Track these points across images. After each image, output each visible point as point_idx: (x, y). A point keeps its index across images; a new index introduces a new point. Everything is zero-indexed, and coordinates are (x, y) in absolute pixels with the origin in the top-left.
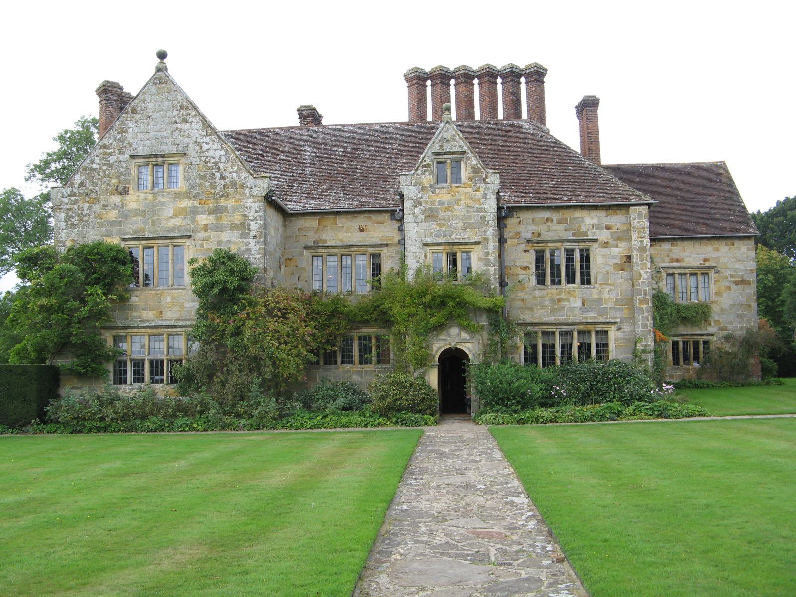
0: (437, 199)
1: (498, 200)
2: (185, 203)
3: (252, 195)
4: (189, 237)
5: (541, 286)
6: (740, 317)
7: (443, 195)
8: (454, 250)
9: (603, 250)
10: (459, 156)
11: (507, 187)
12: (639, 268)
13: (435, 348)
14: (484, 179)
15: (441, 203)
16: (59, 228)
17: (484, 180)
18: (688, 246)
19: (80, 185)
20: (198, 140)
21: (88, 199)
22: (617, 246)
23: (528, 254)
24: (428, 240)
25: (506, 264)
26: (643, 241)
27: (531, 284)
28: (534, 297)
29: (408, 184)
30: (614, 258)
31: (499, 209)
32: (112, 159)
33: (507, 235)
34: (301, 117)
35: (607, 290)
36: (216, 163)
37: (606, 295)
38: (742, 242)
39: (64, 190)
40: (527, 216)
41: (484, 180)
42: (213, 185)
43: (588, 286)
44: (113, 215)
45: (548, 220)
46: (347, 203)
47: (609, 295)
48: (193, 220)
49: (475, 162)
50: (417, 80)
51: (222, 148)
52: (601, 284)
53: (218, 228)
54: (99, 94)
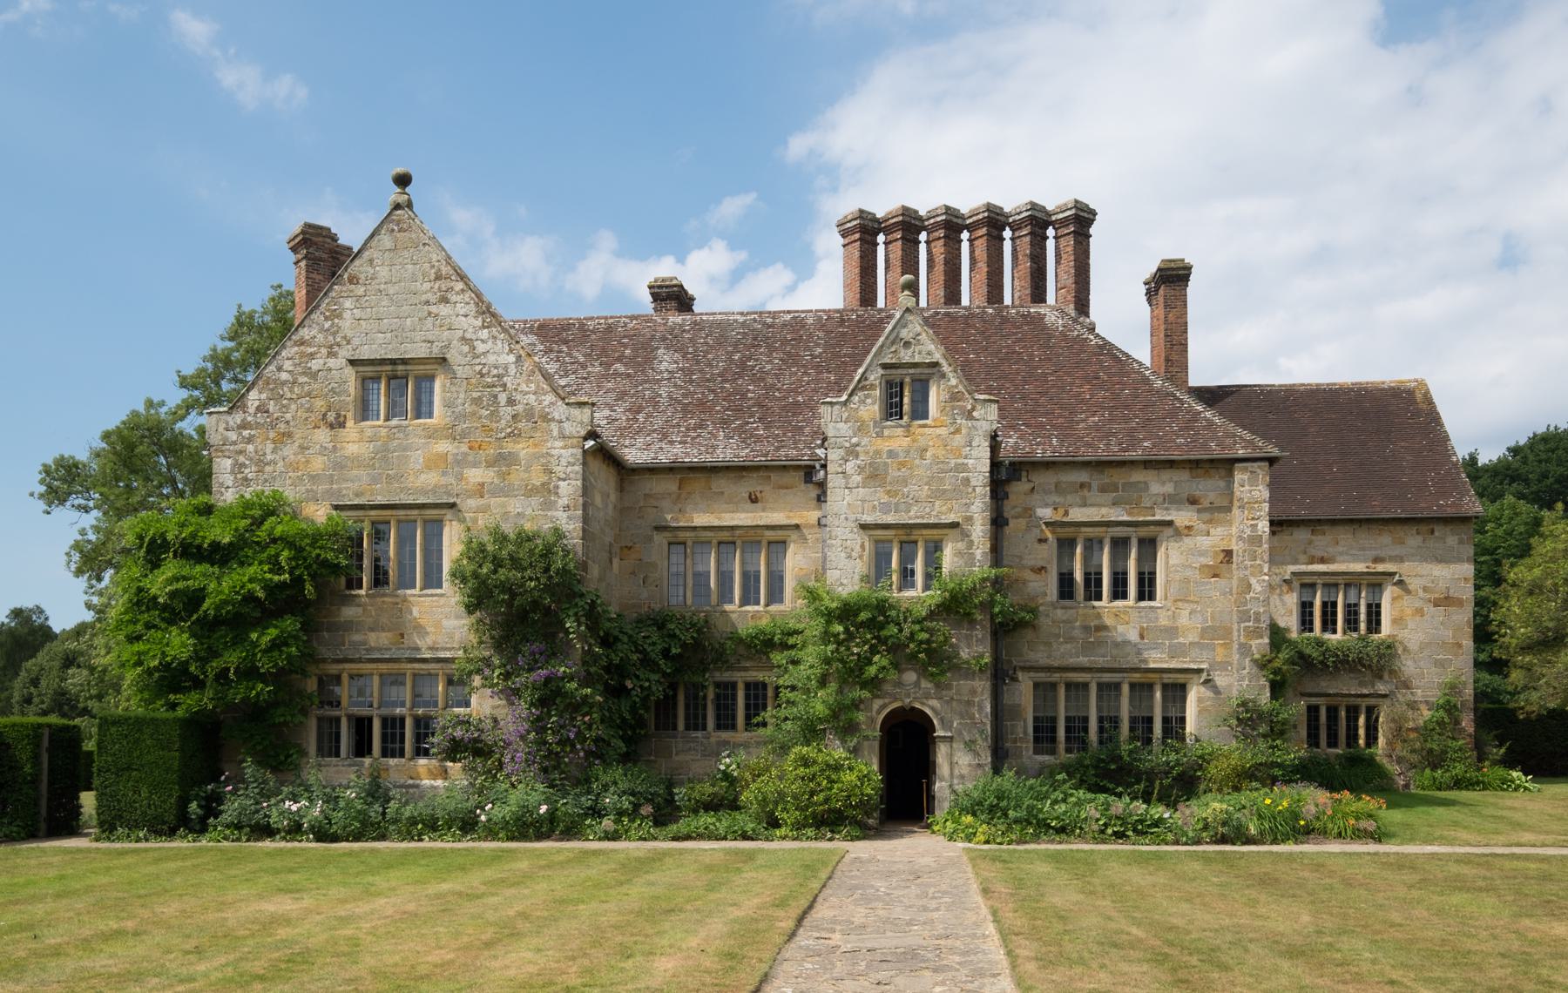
0: (885, 446)
1: (995, 446)
2: (443, 446)
3: (563, 437)
4: (453, 506)
5: (1067, 603)
6: (1440, 664)
7: (896, 438)
10: (927, 371)
11: (1012, 427)
14: (970, 412)
15: (891, 454)
16: (222, 485)
17: (969, 415)
19: (258, 409)
20: (468, 336)
21: (272, 434)
22: (1208, 534)
23: (1045, 546)
24: (868, 519)
27: (1049, 599)
29: (834, 421)
31: (995, 465)
32: (315, 365)
34: (656, 297)
35: (1186, 613)
36: (499, 376)
37: (1184, 620)
38: (1448, 529)
39: (229, 418)
41: (969, 415)
42: (494, 415)
43: (1152, 604)
44: (318, 464)
45: (1082, 485)
46: (727, 450)
47: (1189, 623)
48: (460, 477)
49: (954, 382)
51: (511, 351)
53: (504, 491)
54: (294, 249)
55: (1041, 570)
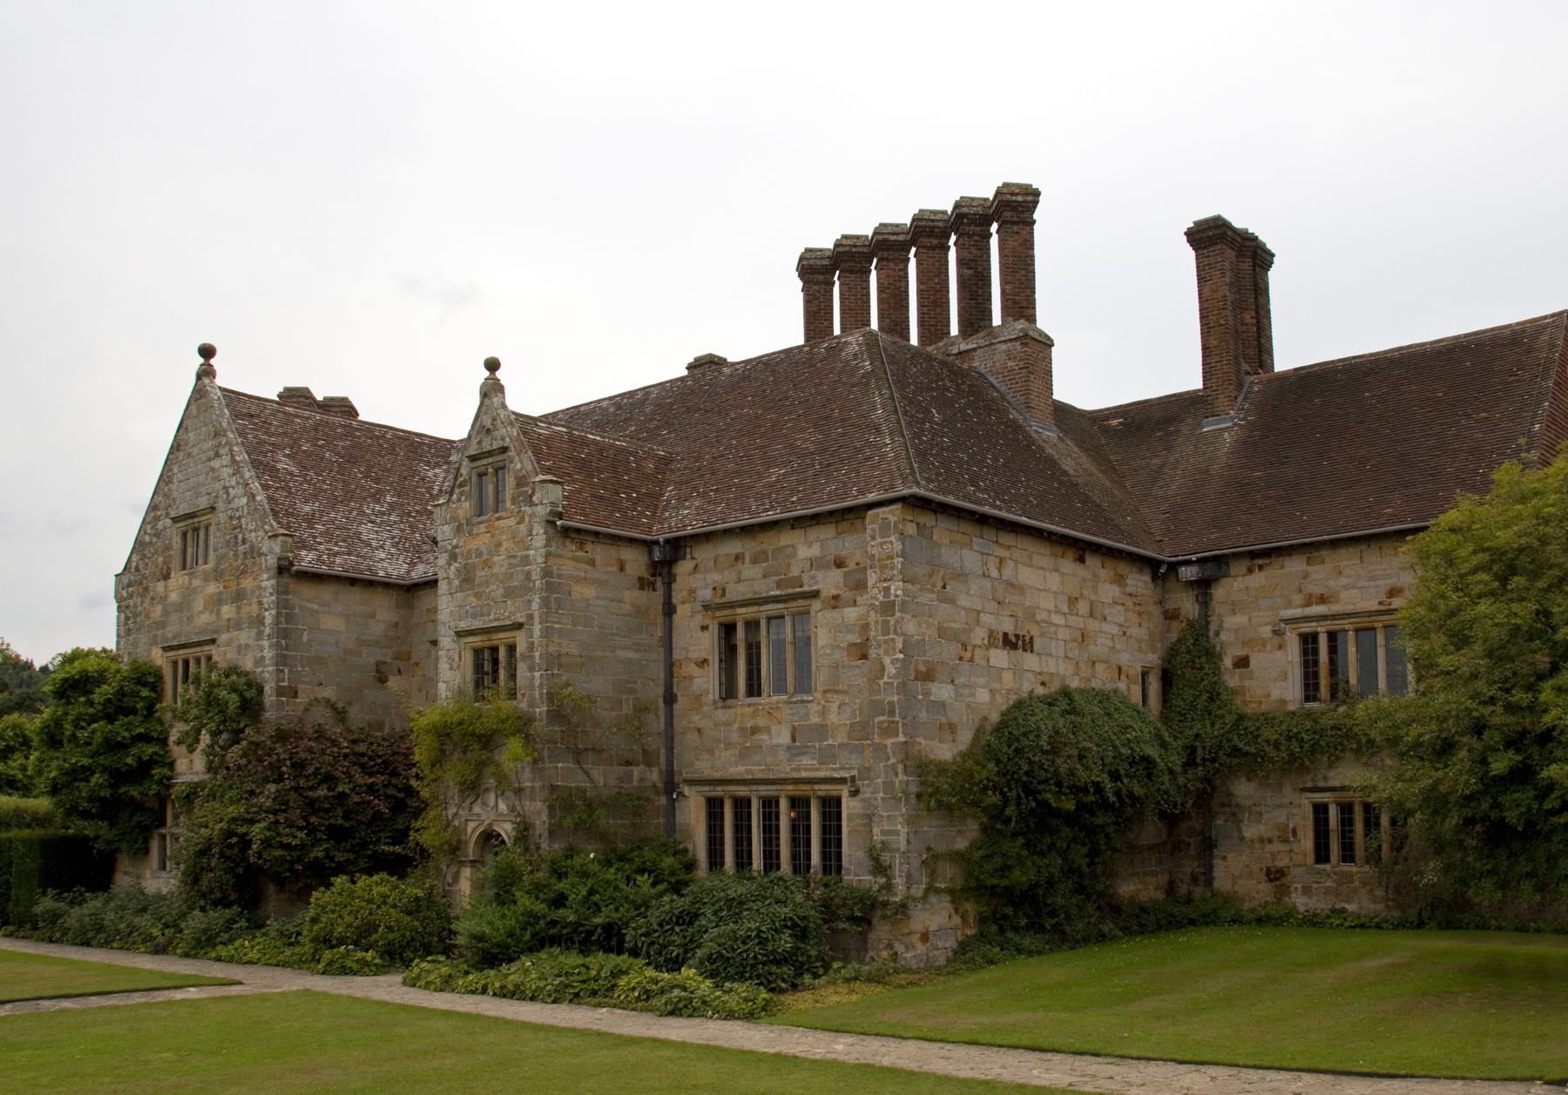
0: (474, 544)
4: (213, 641)
12: (881, 652)
13: (469, 830)
14: (531, 497)
18: (1347, 559)
22: (855, 604)
23: (707, 634)
24: (463, 625)
25: (675, 656)
30: (849, 632)
32: (160, 525)
33: (677, 598)
37: (833, 717)
40: (704, 553)
48: (218, 614)
50: (816, 271)
52: (825, 692)
55: (703, 663)
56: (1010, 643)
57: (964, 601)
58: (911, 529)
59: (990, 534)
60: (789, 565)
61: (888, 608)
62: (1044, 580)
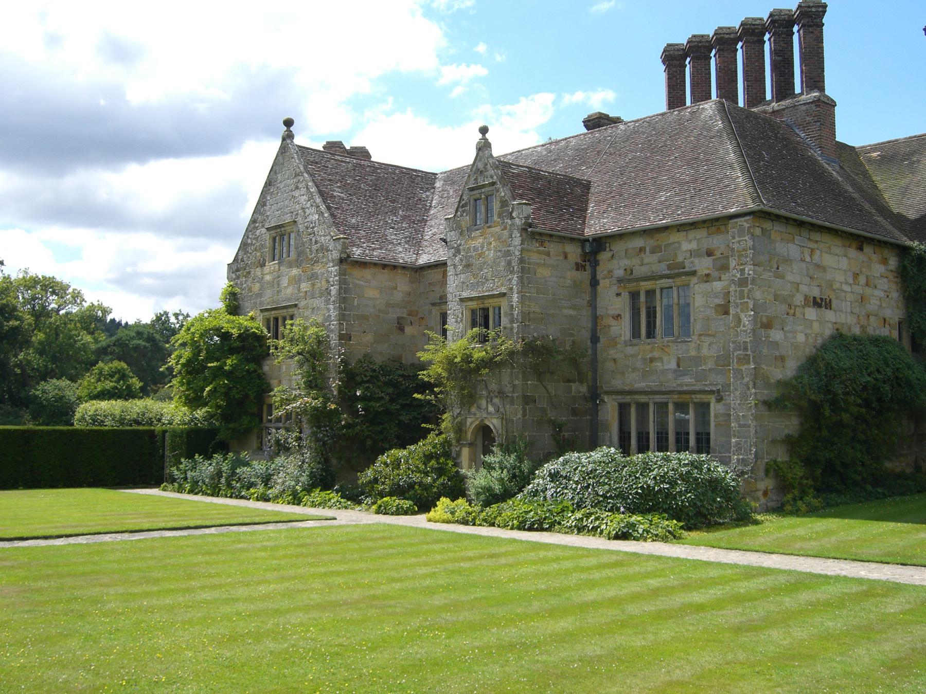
4: (296, 305)
5: (635, 341)
8: (486, 305)
9: (703, 286)
13: (468, 423)
14: (511, 213)
15: (475, 249)
22: (720, 279)
23: (620, 299)
24: (465, 295)
25: (598, 313)
26: (744, 269)
28: (626, 356)
30: (716, 297)
33: (599, 276)
35: (707, 344)
36: (313, 228)
37: (705, 351)
45: (642, 250)
50: (673, 59)
52: (700, 335)
55: (618, 317)
56: (819, 303)
57: (789, 277)
58: (758, 231)
59: (805, 233)
60: (676, 255)
61: (743, 282)
62: (838, 263)
